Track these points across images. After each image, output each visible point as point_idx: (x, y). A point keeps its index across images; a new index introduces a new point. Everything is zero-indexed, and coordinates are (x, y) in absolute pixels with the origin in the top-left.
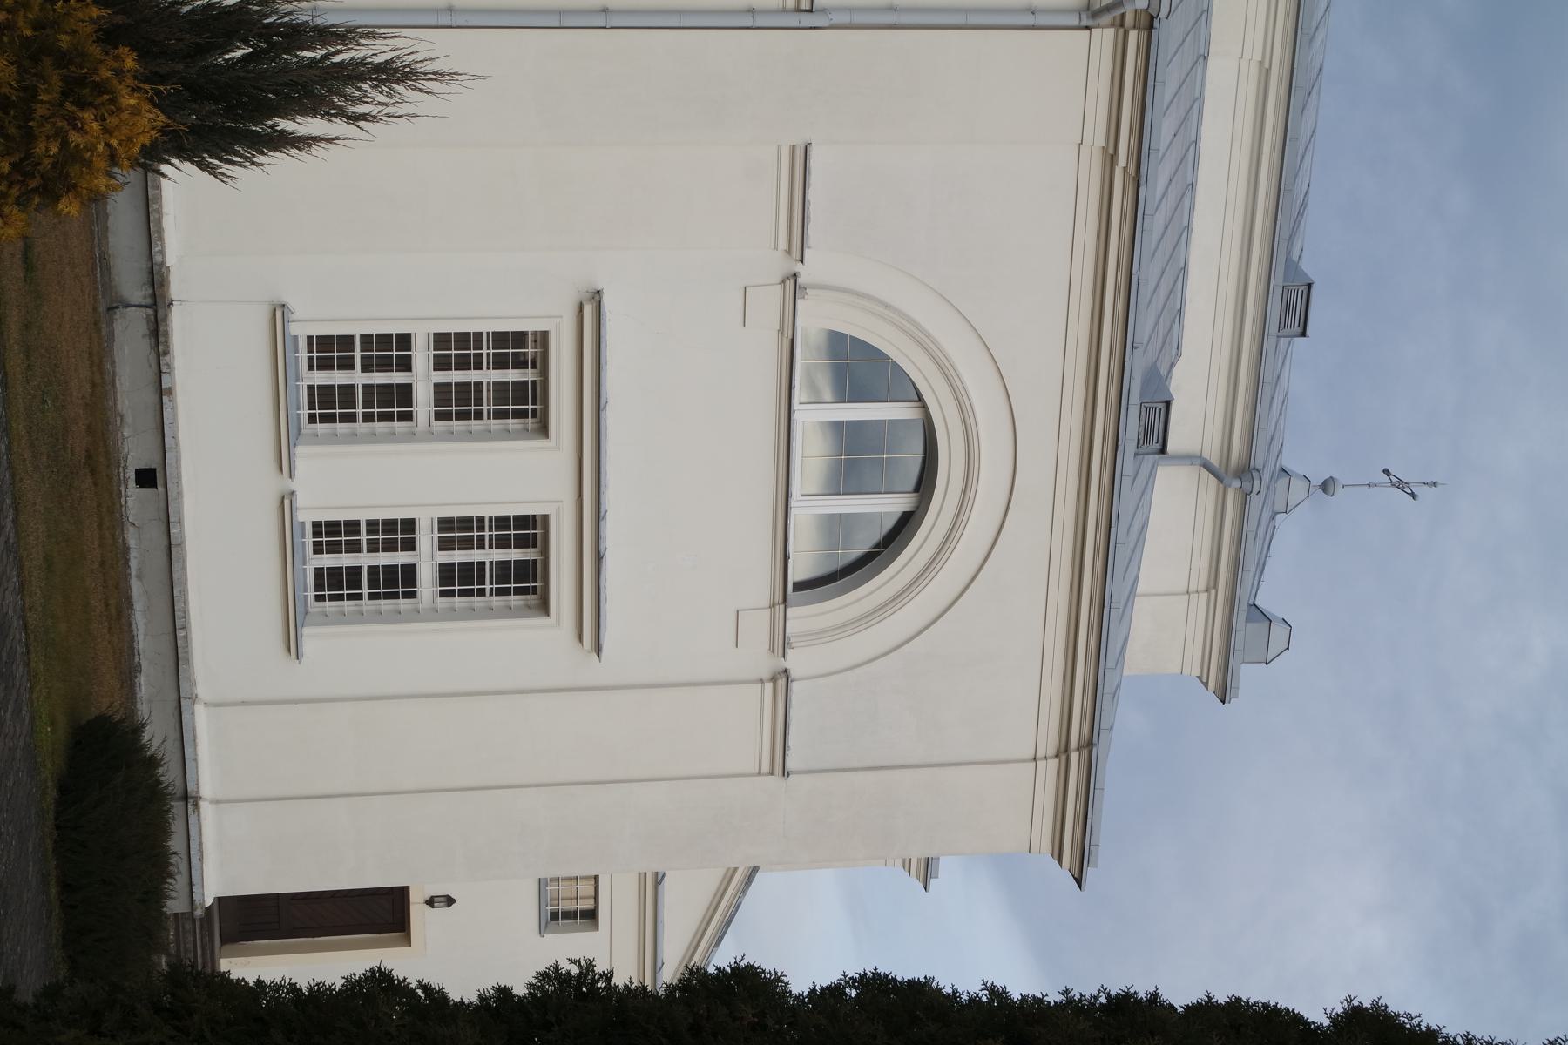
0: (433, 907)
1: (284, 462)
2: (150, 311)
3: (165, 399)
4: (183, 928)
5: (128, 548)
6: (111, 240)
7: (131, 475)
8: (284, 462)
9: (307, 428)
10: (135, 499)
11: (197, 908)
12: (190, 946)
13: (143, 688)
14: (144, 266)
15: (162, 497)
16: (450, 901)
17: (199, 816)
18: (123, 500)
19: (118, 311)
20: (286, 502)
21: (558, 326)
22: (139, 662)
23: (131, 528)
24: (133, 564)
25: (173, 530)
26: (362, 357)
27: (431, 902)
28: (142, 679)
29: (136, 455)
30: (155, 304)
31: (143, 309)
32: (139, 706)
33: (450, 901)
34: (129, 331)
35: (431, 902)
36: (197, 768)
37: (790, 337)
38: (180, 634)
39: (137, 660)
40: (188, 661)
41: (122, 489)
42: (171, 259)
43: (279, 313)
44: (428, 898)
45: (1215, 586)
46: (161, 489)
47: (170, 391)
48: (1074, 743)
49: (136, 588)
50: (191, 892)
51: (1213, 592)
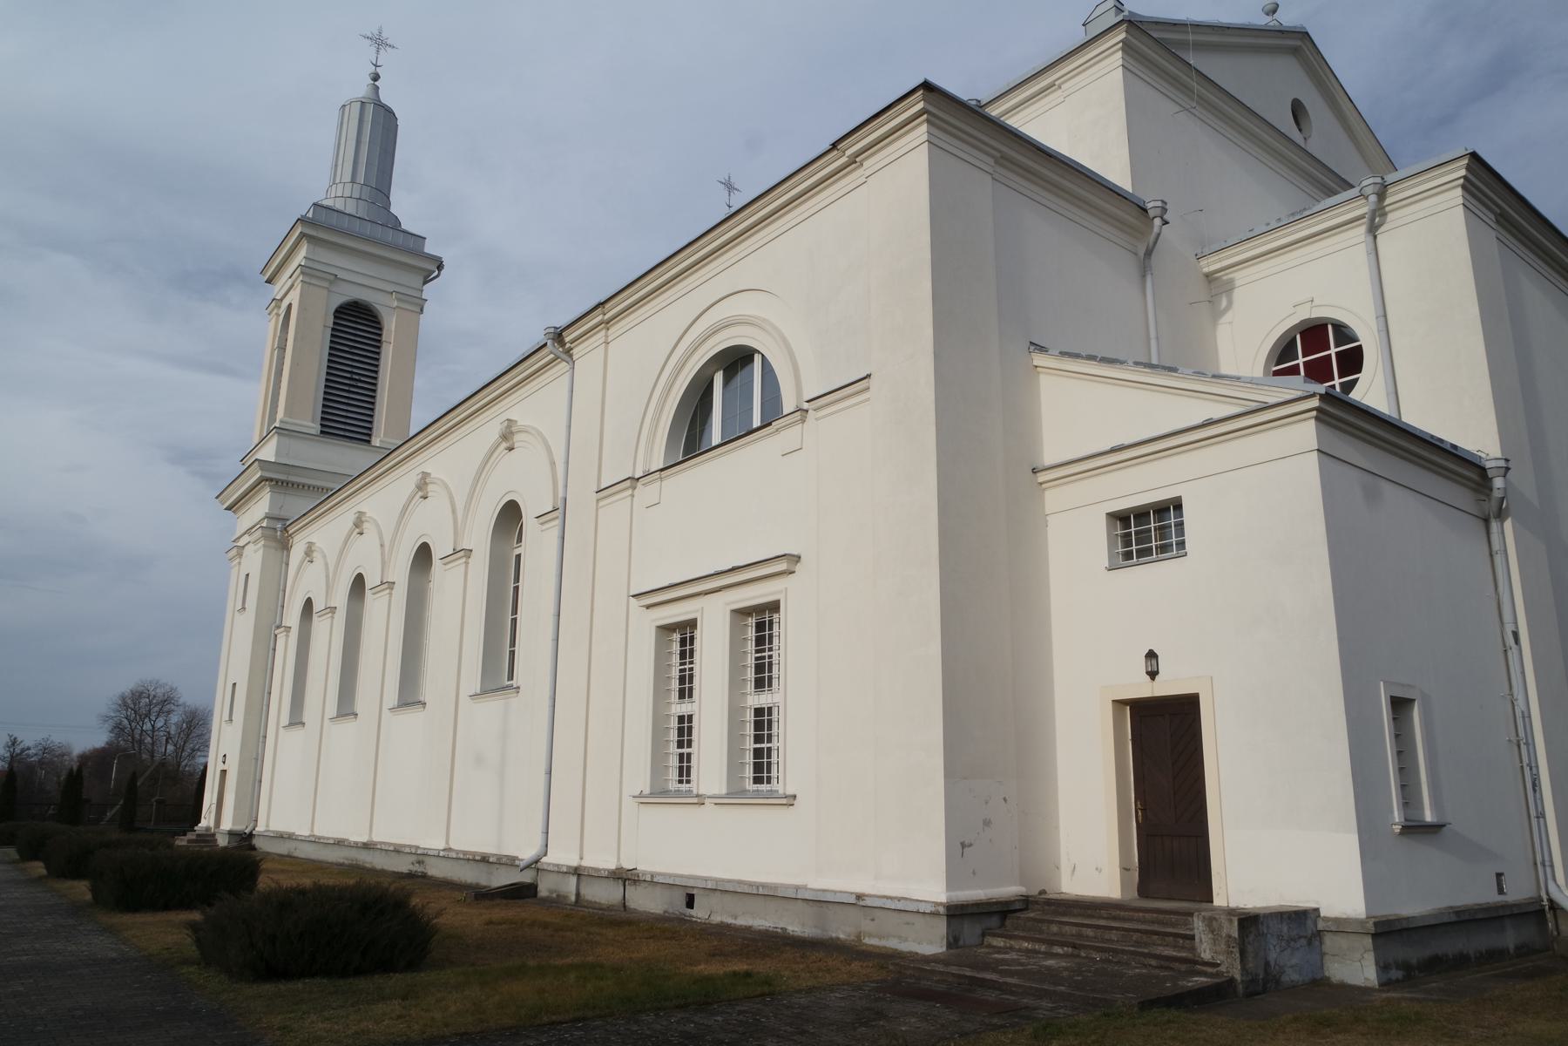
0: (1157, 673)
1: (700, 800)
2: (627, 883)
3: (655, 880)
4: (1055, 934)
5: (722, 922)
6: (603, 902)
7: (689, 910)
8: (700, 800)
9: (693, 785)
10: (699, 913)
11: (938, 911)
12: (1074, 930)
13: (796, 929)
14: (612, 882)
15: (702, 892)
16: (1151, 655)
17: (867, 896)
18: (699, 921)
20: (721, 802)
22: (782, 928)
23: (712, 918)
24: (730, 921)
25: (709, 887)
26: (763, 748)
27: (1153, 675)
31: (627, 887)
32: (806, 935)
33: (1151, 655)
35: (1153, 675)
36: (841, 892)
38: (761, 891)
39: (779, 930)
40: (775, 887)
41: (694, 919)
46: (695, 892)
48: (844, 160)
49: (741, 921)
50: (924, 913)
51: (1057, 83)
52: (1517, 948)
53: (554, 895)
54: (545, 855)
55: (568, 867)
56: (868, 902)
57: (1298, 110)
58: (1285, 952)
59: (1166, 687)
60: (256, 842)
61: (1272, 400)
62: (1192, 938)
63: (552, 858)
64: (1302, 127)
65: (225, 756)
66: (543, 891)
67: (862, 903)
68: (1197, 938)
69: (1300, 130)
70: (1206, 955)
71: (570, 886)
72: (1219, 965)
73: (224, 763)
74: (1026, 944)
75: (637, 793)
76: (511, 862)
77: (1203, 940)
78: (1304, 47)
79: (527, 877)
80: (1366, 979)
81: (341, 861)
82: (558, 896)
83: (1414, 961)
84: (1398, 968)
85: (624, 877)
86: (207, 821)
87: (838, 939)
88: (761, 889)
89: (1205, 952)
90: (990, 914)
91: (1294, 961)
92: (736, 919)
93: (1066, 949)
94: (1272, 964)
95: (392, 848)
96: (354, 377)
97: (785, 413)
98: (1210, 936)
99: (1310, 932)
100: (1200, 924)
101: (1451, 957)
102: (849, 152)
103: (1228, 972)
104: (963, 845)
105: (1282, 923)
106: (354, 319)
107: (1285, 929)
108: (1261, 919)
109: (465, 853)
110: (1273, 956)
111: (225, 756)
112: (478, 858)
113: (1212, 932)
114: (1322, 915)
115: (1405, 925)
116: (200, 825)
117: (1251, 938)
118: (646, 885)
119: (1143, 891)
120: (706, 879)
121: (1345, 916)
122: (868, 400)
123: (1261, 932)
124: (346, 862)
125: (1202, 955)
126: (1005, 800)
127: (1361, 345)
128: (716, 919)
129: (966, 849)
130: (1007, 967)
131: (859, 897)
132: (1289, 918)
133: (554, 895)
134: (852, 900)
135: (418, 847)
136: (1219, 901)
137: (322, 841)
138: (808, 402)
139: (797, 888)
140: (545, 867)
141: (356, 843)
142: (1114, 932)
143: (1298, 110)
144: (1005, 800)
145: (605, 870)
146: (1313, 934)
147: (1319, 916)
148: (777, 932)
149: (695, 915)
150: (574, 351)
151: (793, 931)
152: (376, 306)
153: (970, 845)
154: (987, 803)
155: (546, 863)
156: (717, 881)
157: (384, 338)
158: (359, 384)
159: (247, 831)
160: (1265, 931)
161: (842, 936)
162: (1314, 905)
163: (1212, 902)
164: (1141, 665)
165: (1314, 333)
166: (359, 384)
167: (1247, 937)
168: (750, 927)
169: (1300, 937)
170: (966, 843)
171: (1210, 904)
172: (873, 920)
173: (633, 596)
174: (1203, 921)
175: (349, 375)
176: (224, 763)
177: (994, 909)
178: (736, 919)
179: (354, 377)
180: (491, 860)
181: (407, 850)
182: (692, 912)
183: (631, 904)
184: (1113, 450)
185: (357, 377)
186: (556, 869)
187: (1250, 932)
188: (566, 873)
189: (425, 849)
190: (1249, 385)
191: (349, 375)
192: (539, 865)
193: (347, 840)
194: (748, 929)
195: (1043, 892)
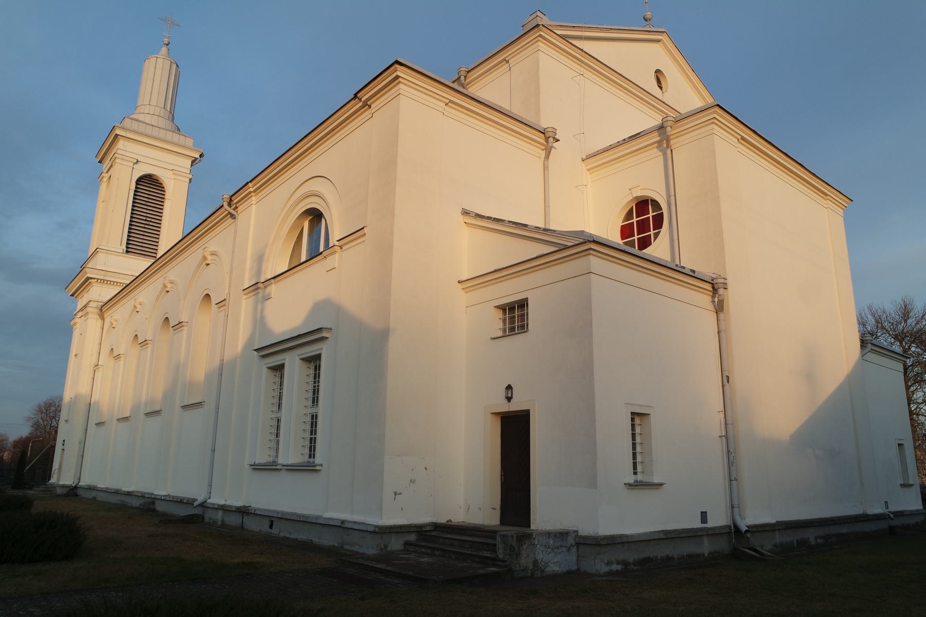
2: (244, 515)
3: (256, 513)
5: (284, 537)
6: (233, 525)
7: (270, 529)
10: (275, 531)
11: (375, 530)
13: (316, 540)
19: (244, 526)
21: (266, 364)
22: (310, 540)
23: (280, 534)
24: (288, 536)
27: (509, 399)
28: (314, 540)
29: (264, 526)
30: (241, 512)
31: (244, 517)
33: (509, 387)
34: (252, 525)
35: (509, 399)
37: (272, 280)
38: (302, 519)
39: (309, 541)
42: (239, 503)
43: (257, 468)
44: (506, 401)
45: (504, 60)
46: (273, 519)
47: (255, 510)
49: (293, 536)
50: (370, 532)
52: (710, 553)
53: (211, 521)
54: (210, 498)
55: (218, 505)
56: (347, 525)
57: (659, 76)
58: (550, 554)
59: (515, 406)
60: (80, 492)
61: (570, 244)
62: (495, 545)
63: (216, 500)
64: (663, 85)
65: (64, 441)
66: (206, 520)
67: (343, 526)
68: (497, 546)
69: (661, 88)
70: (501, 556)
71: (219, 515)
72: (506, 561)
73: (63, 445)
74: (423, 550)
75: (253, 463)
76: (190, 502)
77: (500, 547)
78: (664, 39)
79: (198, 511)
80: (596, 570)
81: (117, 502)
82: (213, 522)
83: (631, 560)
84: (618, 563)
85: (243, 511)
86: (53, 480)
87: (334, 546)
88: (301, 518)
89: (500, 554)
90: (410, 532)
91: (556, 560)
92: (290, 534)
93: (440, 552)
94: (539, 561)
95: (140, 495)
96: (148, 219)
97: (330, 246)
98: (503, 545)
99: (570, 544)
100: (499, 539)
101: (659, 558)
102: (363, 99)
103: (509, 565)
104: (396, 494)
105: (549, 538)
106: (148, 185)
107: (551, 542)
108: (534, 537)
109: (173, 497)
110: (540, 556)
111: (64, 441)
112: (179, 500)
113: (504, 544)
114: (579, 534)
115: (625, 540)
116: (50, 481)
117: (525, 547)
118: (252, 515)
119: (504, 521)
120: (278, 512)
121: (589, 535)
122: (364, 241)
123: (533, 543)
124: (119, 503)
125: (499, 557)
126: (426, 468)
127: (663, 213)
128: (282, 534)
129: (397, 496)
130: (398, 562)
131: (343, 522)
132: (555, 536)
133: (211, 521)
134: (339, 524)
135: (152, 494)
136: (533, 527)
137: (108, 491)
138: (338, 241)
139: (318, 517)
140: (210, 506)
141: (124, 492)
142: (468, 543)
143: (659, 76)
144: (426, 468)
145: (235, 507)
146: (572, 545)
147: (578, 535)
148: (308, 542)
149: (273, 532)
150: (239, 208)
151: (315, 542)
152: (162, 178)
153: (401, 494)
154: (413, 470)
155: (209, 503)
156: (283, 513)
157: (166, 197)
158: (151, 224)
159: (74, 485)
160: (536, 543)
161: (336, 544)
162: (575, 529)
163: (529, 526)
164: (502, 393)
165: (643, 205)
166: (151, 224)
167: (522, 546)
168: (297, 539)
169: (561, 546)
170: (398, 493)
171: (528, 529)
172: (348, 535)
173: (255, 350)
174: (500, 537)
175: (144, 218)
176: (63, 445)
177: (412, 529)
178: (290, 534)
179: (148, 219)
180: (185, 501)
181: (147, 496)
182: (272, 531)
183: (245, 526)
184: (495, 271)
185: (149, 219)
186: (212, 506)
187: (525, 543)
188: (217, 509)
189: (155, 495)
190: (559, 235)
191: (144, 218)
192: (205, 504)
193: (120, 490)
194: (296, 540)
195: (450, 521)
